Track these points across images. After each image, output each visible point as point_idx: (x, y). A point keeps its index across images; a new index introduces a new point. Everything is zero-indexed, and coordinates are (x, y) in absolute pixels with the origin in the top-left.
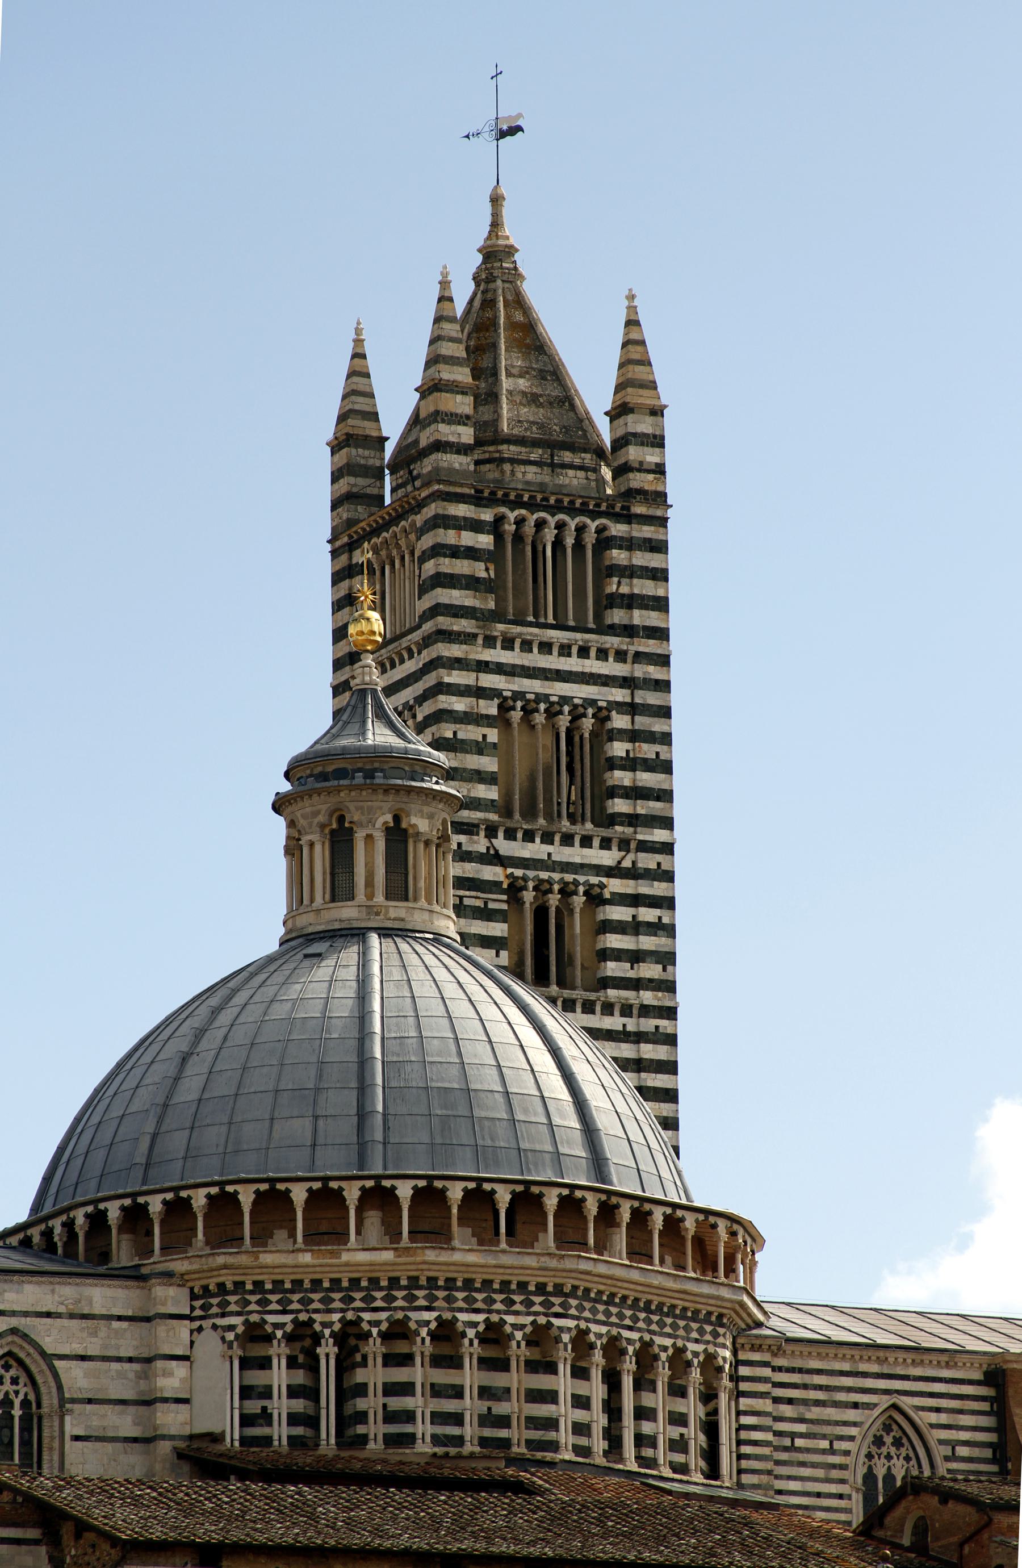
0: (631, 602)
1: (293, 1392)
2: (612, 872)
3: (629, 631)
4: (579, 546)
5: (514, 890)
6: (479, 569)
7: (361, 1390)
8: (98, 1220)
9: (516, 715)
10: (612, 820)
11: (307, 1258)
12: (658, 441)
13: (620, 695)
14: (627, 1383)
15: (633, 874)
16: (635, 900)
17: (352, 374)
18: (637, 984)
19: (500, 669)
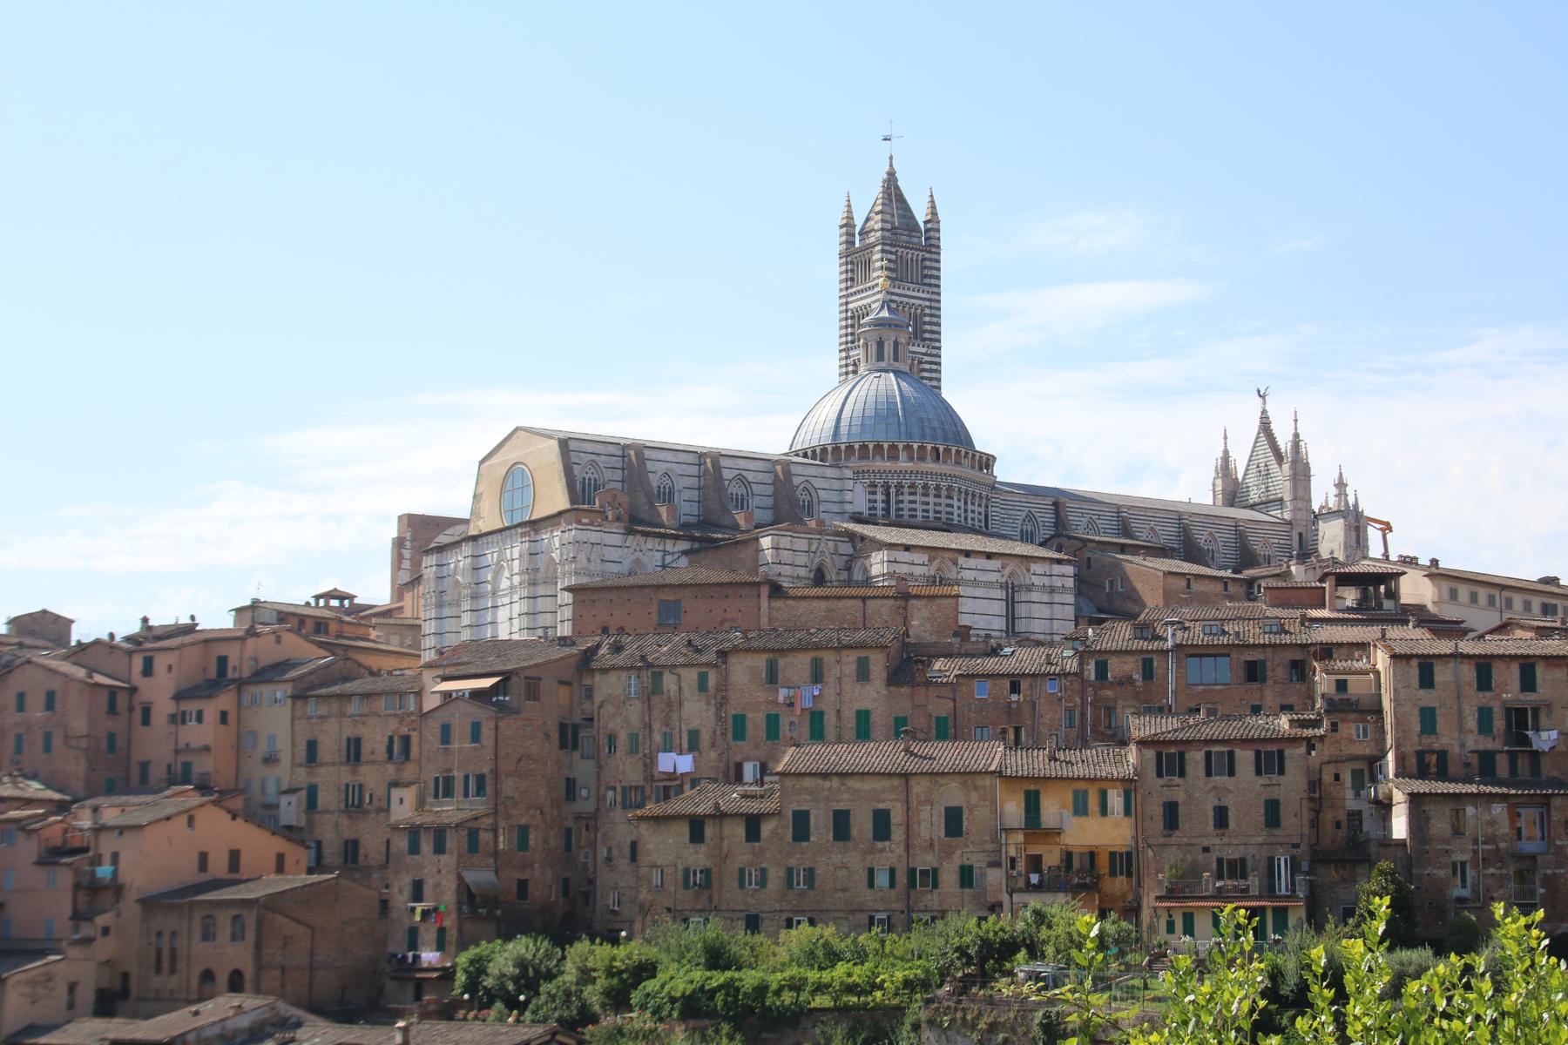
0: (931, 277)
1: (883, 502)
2: (925, 354)
3: (930, 285)
4: (917, 260)
7: (902, 502)
10: (925, 339)
11: (888, 464)
12: (938, 230)
13: (928, 303)
14: (969, 502)
16: (931, 363)
19: (897, 295)
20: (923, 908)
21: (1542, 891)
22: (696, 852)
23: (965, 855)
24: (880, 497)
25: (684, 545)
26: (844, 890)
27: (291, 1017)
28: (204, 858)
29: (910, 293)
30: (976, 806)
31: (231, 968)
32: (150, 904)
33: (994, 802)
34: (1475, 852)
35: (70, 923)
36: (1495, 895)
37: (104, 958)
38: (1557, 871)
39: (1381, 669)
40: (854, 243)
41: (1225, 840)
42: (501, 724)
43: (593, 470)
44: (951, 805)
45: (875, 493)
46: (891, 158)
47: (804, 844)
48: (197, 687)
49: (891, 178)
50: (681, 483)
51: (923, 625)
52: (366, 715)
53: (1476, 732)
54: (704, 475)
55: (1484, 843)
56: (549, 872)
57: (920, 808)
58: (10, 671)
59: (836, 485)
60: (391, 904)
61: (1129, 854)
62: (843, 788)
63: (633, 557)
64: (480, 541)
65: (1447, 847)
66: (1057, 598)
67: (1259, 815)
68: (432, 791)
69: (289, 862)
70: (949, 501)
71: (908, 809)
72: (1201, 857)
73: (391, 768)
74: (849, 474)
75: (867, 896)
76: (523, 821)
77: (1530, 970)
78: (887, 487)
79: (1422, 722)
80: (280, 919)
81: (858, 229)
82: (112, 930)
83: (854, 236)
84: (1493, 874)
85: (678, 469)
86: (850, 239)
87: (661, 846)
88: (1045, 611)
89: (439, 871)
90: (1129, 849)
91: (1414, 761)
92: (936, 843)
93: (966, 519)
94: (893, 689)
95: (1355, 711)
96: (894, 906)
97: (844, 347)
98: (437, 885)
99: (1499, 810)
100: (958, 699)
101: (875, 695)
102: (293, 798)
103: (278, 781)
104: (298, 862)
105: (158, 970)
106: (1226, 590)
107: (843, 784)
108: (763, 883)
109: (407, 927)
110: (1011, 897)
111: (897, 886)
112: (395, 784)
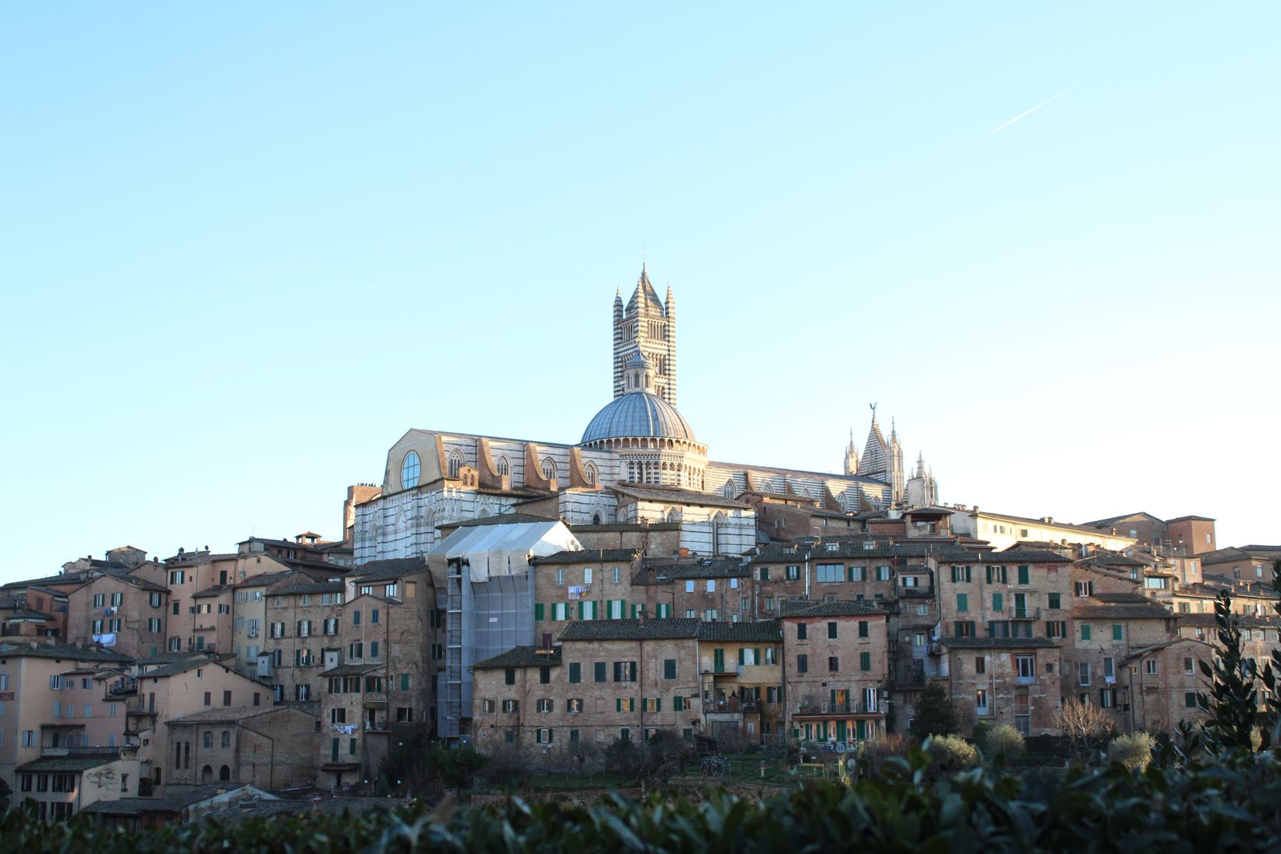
7: (650, 473)
8: (602, 442)
9: (651, 355)
14: (692, 474)
20: (651, 724)
21: (1032, 708)
22: (510, 690)
23: (677, 691)
24: (636, 471)
25: (513, 501)
26: (602, 713)
27: (255, 795)
28: (208, 695)
29: (657, 346)
30: (683, 659)
31: (222, 765)
32: (172, 725)
33: (694, 656)
34: (991, 684)
35: (124, 737)
36: (1003, 711)
37: (145, 760)
38: (1041, 696)
39: (934, 571)
41: (836, 678)
42: (391, 611)
43: (457, 455)
44: (668, 659)
45: (633, 468)
46: (644, 264)
47: (578, 684)
48: (208, 590)
50: (511, 463)
51: (657, 548)
52: (311, 607)
53: (992, 609)
54: (527, 458)
55: (997, 678)
56: (422, 704)
57: (649, 660)
58: (94, 581)
59: (609, 463)
60: (322, 724)
61: (779, 689)
62: (601, 649)
63: (481, 508)
64: (388, 499)
65: (974, 681)
66: (744, 532)
67: (857, 662)
68: (349, 653)
69: (262, 699)
71: (642, 661)
72: (821, 689)
73: (326, 640)
74: (616, 456)
75: (616, 717)
76: (405, 672)
77: (195, 726)
78: (640, 464)
79: (959, 603)
80: (252, 733)
81: (624, 308)
82: (150, 742)
83: (622, 311)
84: (1002, 698)
86: (620, 313)
87: (488, 687)
88: (736, 540)
89: (352, 703)
90: (779, 685)
91: (954, 627)
92: (659, 683)
94: (635, 587)
95: (916, 597)
96: (633, 722)
97: (616, 379)
98: (351, 712)
99: (1005, 658)
100: (675, 592)
101: (624, 591)
102: (266, 659)
103: (257, 648)
104: (268, 698)
105: (178, 766)
106: (849, 525)
107: (601, 646)
108: (550, 708)
109: (332, 738)
110: (706, 716)
111: (635, 709)
112: (329, 650)
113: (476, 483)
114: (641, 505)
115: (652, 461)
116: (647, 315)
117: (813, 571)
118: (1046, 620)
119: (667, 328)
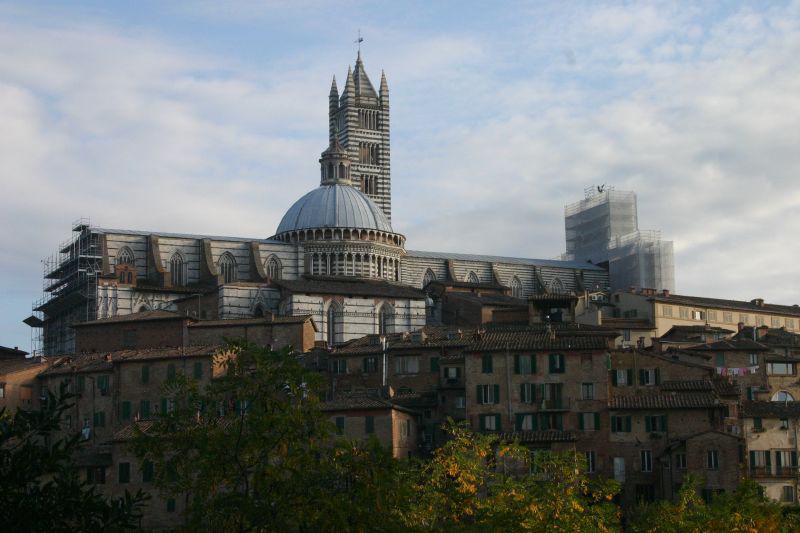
3: (382, 130)
5: (362, 176)
6: (356, 119)
8: (288, 235)
13: (380, 142)
15: (383, 174)
17: (333, 88)
18: (383, 194)
24: (320, 262)
40: (337, 106)
49: (359, 64)
70: (366, 264)
85: (185, 250)
93: (379, 273)
113: (134, 280)
114: (296, 298)
115: (337, 253)
116: (357, 105)
117: (390, 362)
118: (578, 411)
119: (381, 117)
